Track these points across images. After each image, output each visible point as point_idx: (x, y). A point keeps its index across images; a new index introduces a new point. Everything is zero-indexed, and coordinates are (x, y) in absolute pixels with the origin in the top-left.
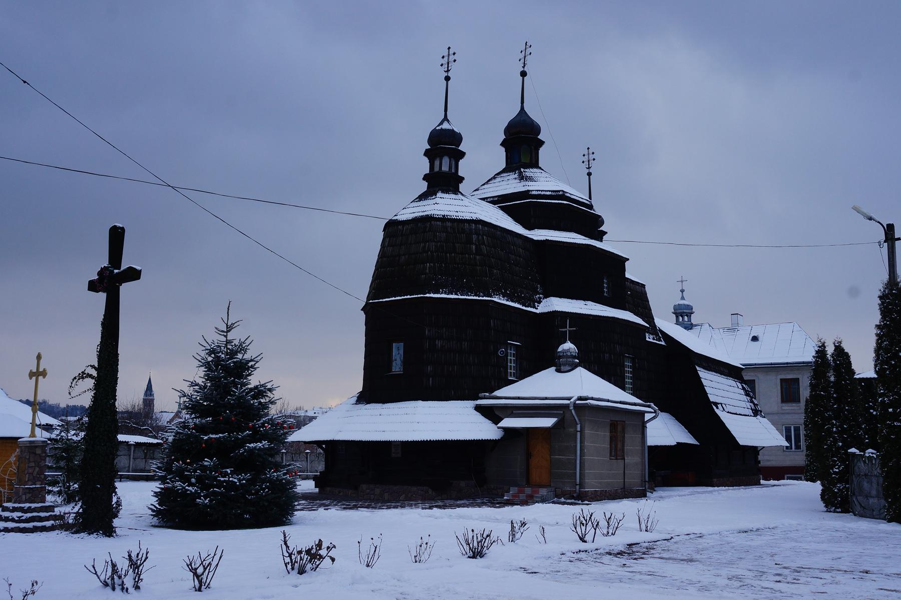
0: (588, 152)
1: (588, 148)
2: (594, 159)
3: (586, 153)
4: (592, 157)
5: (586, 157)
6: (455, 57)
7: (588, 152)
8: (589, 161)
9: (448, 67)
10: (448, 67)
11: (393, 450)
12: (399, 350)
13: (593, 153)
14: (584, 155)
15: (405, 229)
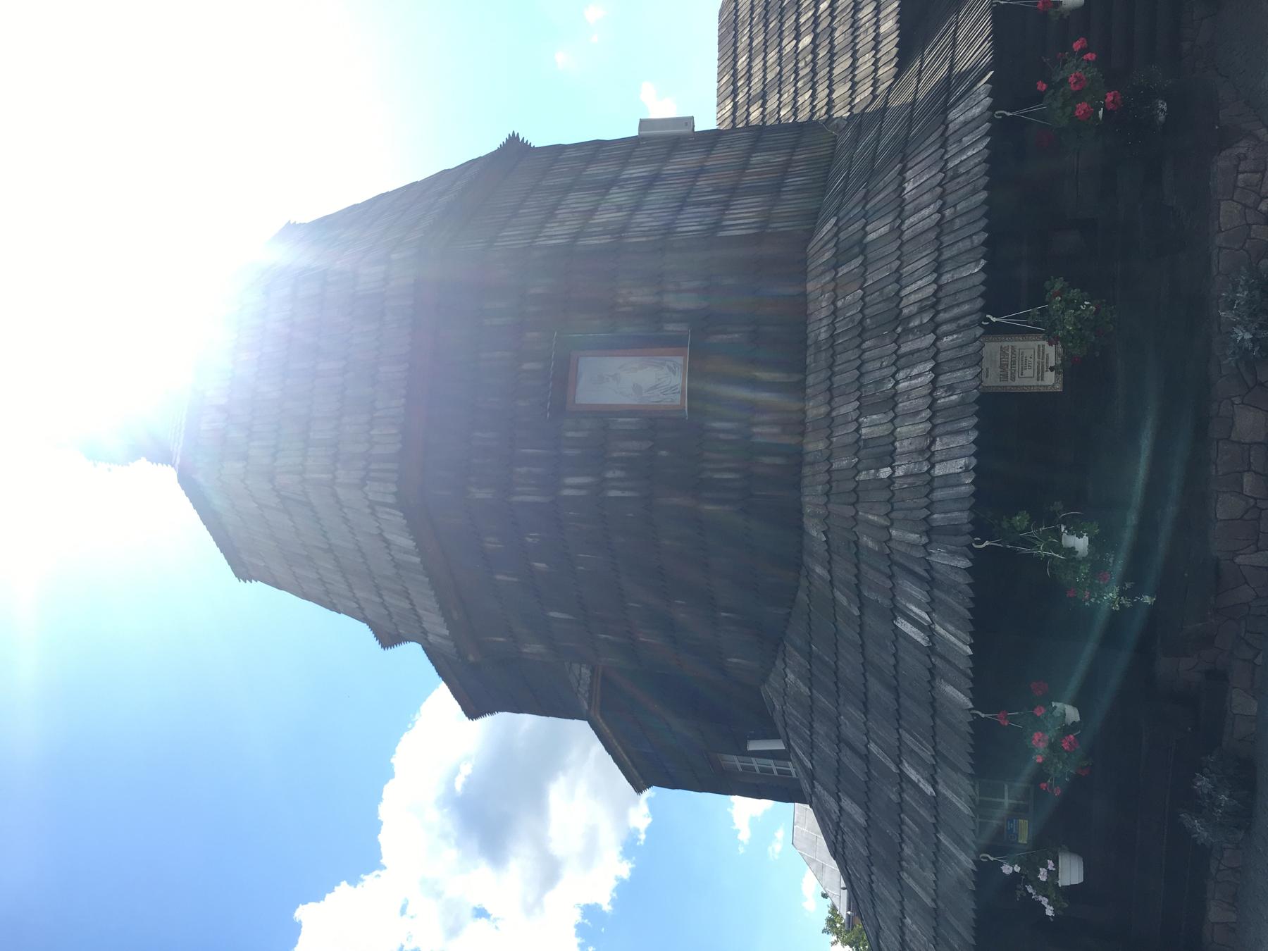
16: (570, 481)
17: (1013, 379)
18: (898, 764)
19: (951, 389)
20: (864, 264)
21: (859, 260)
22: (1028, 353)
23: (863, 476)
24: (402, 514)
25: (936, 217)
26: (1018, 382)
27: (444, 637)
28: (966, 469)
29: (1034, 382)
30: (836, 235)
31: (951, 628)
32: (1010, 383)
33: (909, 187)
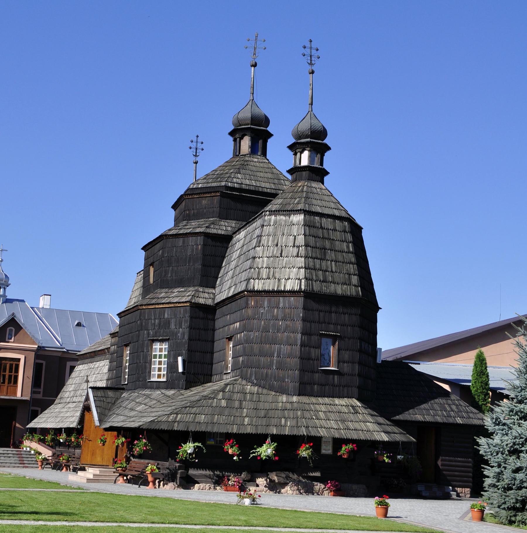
0: (197, 139)
1: (198, 136)
2: (203, 150)
3: (195, 139)
4: (200, 146)
5: (194, 144)
6: (318, 53)
7: (197, 139)
8: (196, 149)
9: (311, 60)
10: (311, 60)
11: (323, 447)
12: (327, 345)
13: (202, 143)
14: (192, 142)
15: (323, 222)
16: (306, 337)
17: (324, 444)
18: (246, 416)
19: (334, 432)
20: (353, 413)
21: (353, 411)
22: (329, 447)
23: (312, 412)
24: (298, 290)
25: (364, 430)
26: (323, 445)
27: (254, 287)
28: (322, 435)
29: (323, 448)
30: (358, 406)
31: (289, 430)
32: (323, 443)
33: (369, 424)
